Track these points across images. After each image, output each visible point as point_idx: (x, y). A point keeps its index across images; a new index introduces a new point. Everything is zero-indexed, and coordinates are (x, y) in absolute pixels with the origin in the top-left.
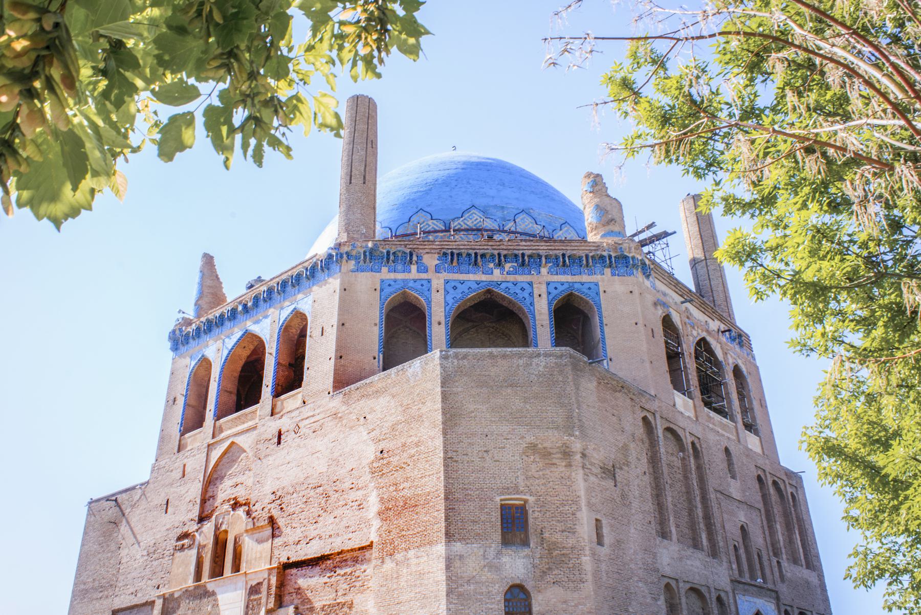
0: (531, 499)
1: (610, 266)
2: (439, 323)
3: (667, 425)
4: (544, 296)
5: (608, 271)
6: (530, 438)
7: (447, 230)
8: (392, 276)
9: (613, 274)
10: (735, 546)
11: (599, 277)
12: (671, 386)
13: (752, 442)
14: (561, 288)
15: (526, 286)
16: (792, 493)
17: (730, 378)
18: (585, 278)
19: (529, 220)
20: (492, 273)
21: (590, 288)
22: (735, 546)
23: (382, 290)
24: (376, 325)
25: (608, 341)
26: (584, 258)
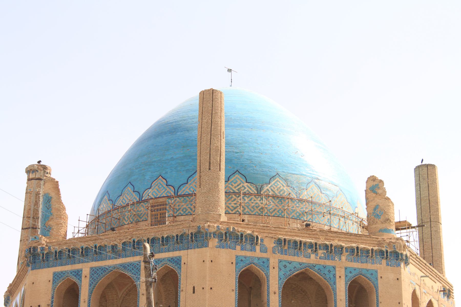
4: (343, 277)
5: (384, 261)
7: (259, 194)
8: (243, 253)
9: (388, 265)
11: (378, 265)
14: (354, 273)
15: (332, 269)
18: (369, 266)
19: (316, 190)
20: (310, 257)
21: (372, 274)
23: (237, 264)
24: (233, 290)
26: (370, 252)
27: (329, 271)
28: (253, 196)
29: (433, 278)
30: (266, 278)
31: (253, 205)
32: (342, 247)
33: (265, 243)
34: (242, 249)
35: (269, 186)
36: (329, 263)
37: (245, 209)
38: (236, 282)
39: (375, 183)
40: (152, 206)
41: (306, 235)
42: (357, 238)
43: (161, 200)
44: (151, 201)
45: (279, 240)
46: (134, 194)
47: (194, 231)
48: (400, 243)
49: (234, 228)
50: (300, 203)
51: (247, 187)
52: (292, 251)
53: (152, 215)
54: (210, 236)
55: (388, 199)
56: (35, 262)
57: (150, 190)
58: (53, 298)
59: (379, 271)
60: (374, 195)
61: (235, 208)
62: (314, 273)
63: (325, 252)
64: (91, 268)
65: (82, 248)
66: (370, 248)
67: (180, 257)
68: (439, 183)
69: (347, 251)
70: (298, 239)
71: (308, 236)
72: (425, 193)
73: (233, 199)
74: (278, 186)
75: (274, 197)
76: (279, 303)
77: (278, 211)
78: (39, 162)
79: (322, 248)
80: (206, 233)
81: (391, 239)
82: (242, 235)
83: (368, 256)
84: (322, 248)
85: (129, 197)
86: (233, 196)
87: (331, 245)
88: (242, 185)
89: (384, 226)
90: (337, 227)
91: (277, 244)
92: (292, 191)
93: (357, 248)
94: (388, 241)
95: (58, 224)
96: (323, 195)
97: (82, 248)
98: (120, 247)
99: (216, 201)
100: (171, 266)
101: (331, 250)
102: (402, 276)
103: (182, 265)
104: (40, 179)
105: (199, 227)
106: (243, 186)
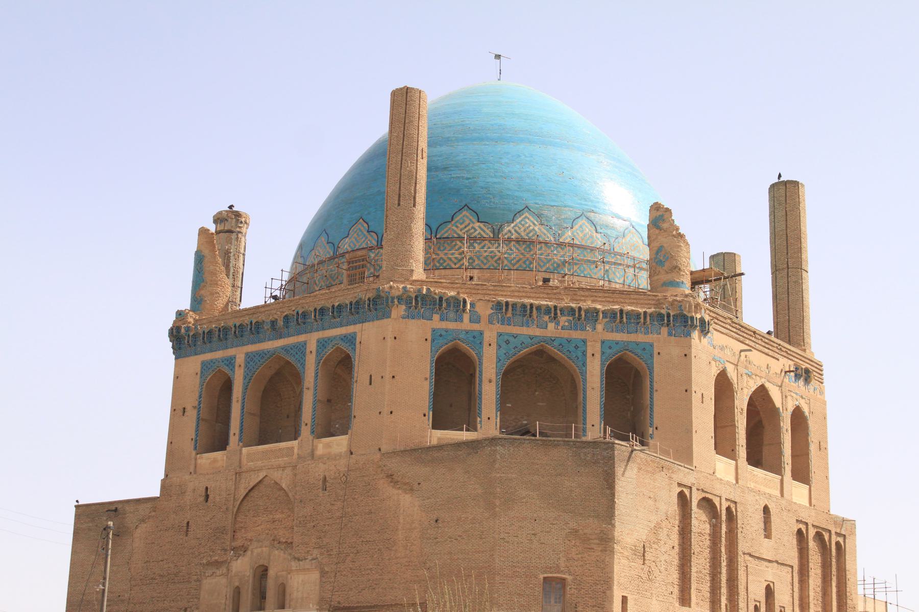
0: (569, 578)
1: (668, 325)
2: (490, 381)
3: (704, 495)
5: (664, 330)
6: (573, 525)
7: (495, 238)
8: (444, 325)
9: (670, 334)
10: (756, 606)
11: (655, 336)
12: (714, 452)
13: (798, 493)
14: (616, 348)
16: (838, 543)
17: (786, 424)
18: (641, 338)
19: (588, 228)
21: (644, 349)
22: (756, 606)
23: (433, 340)
24: (426, 379)
25: (656, 409)
26: (642, 316)
27: (576, 347)
28: (487, 242)
29: (771, 353)
30: (476, 358)
31: (486, 254)
32: (597, 311)
33: (477, 309)
34: (442, 320)
35: (512, 225)
36: (576, 335)
37: (474, 261)
38: (431, 367)
39: (659, 213)
40: (349, 263)
41: (542, 295)
42: (624, 296)
43: (360, 253)
44: (347, 255)
45: (499, 303)
46: (328, 246)
47: (370, 295)
48: (690, 302)
49: (428, 289)
50: (559, 249)
51: (479, 229)
52: (518, 319)
53: (348, 276)
54: (393, 302)
55: (681, 236)
56: (180, 348)
57: (347, 240)
58: (200, 397)
59: (655, 344)
60: (657, 232)
61: (460, 260)
62: (553, 350)
63: (571, 318)
64: (247, 354)
65: (235, 326)
66: (641, 310)
67: (355, 333)
68: (807, 208)
69: (605, 316)
70: (527, 301)
71: (545, 296)
72: (781, 226)
73: (457, 247)
74: (528, 225)
75: (517, 241)
76: (497, 395)
77: (524, 263)
78: (231, 207)
79: (566, 313)
80: (387, 298)
81: (676, 296)
82: (441, 299)
83: (638, 323)
84: (566, 313)
85: (324, 252)
86: (458, 243)
87: (580, 309)
88: (471, 225)
89: (669, 277)
90: (621, 281)
91: (496, 309)
92: (548, 231)
93: (621, 311)
94: (670, 299)
95: (212, 294)
96: (599, 236)
97: (235, 326)
98: (281, 323)
99: (407, 251)
100: (344, 346)
101: (580, 315)
102: (693, 350)
103: (358, 345)
104: (231, 232)
105: (378, 289)
106: (473, 228)
